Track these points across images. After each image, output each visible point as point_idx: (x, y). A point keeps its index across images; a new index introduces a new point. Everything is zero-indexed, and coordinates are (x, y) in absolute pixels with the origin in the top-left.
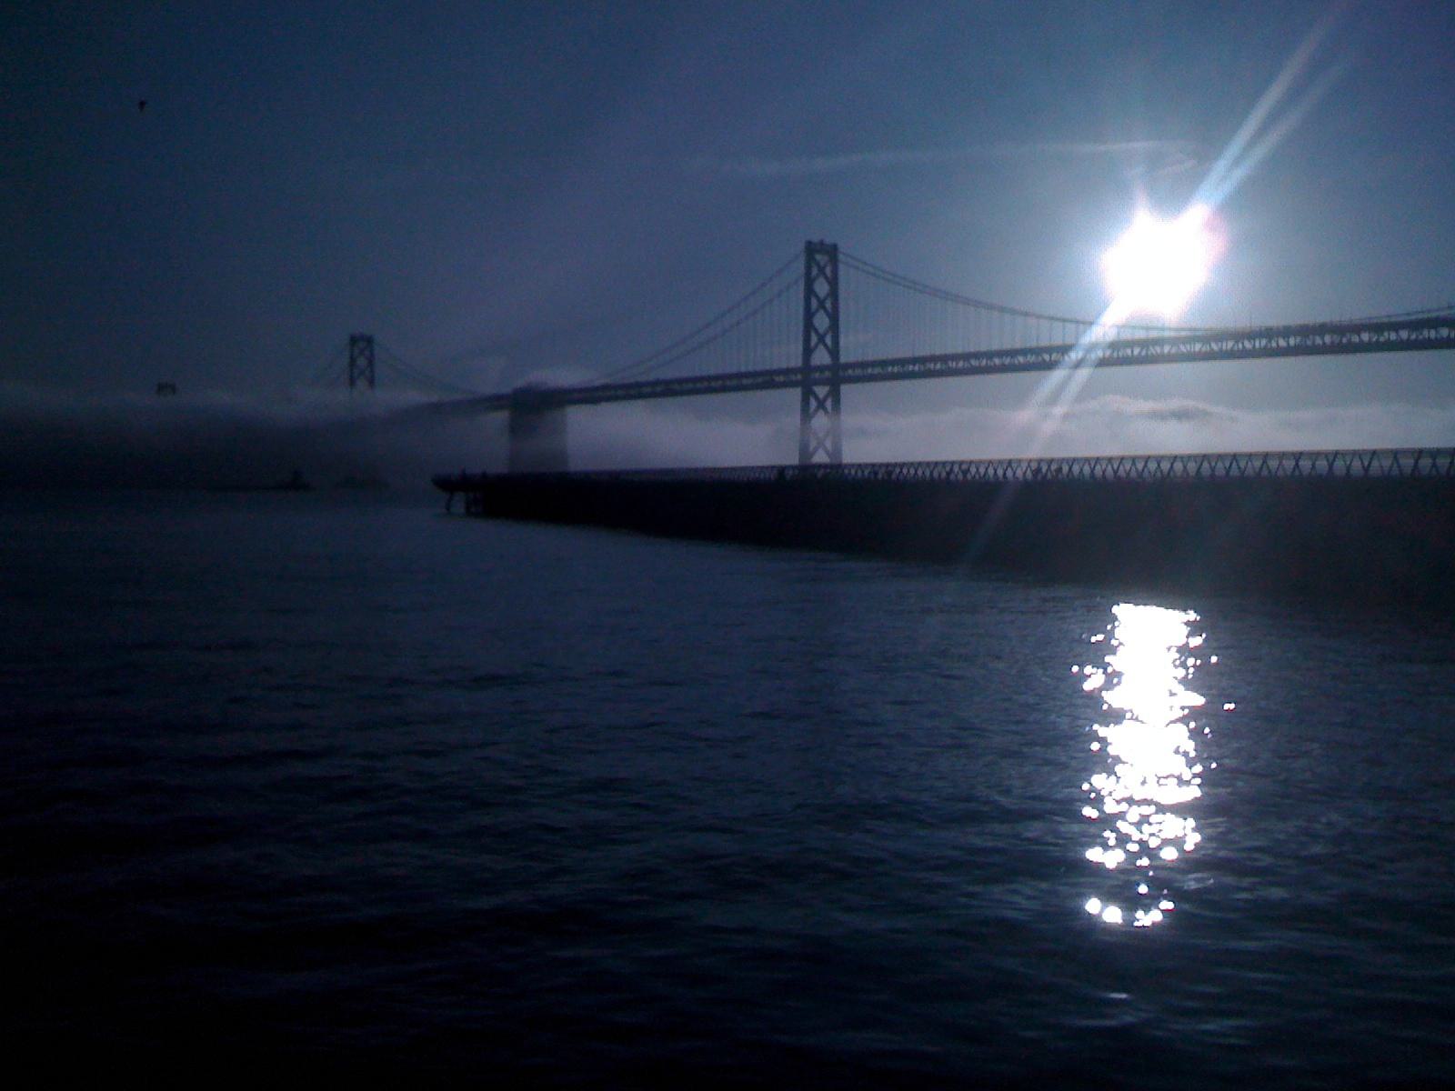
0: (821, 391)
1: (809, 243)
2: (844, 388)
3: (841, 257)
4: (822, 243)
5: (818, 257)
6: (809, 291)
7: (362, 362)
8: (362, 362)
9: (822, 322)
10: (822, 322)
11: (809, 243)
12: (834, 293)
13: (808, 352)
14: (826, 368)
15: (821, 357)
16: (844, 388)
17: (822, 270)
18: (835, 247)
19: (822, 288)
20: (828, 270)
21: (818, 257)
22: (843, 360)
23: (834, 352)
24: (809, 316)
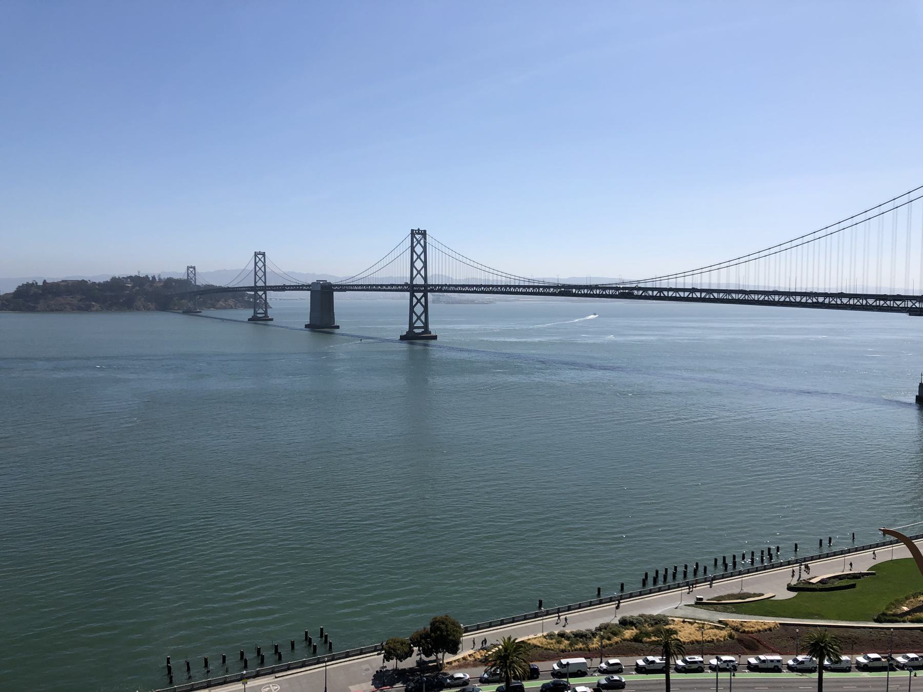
0: (419, 295)
7: (260, 264)
8: (260, 264)
13: (412, 278)
14: (421, 286)
15: (419, 281)
22: (429, 282)
23: (425, 279)
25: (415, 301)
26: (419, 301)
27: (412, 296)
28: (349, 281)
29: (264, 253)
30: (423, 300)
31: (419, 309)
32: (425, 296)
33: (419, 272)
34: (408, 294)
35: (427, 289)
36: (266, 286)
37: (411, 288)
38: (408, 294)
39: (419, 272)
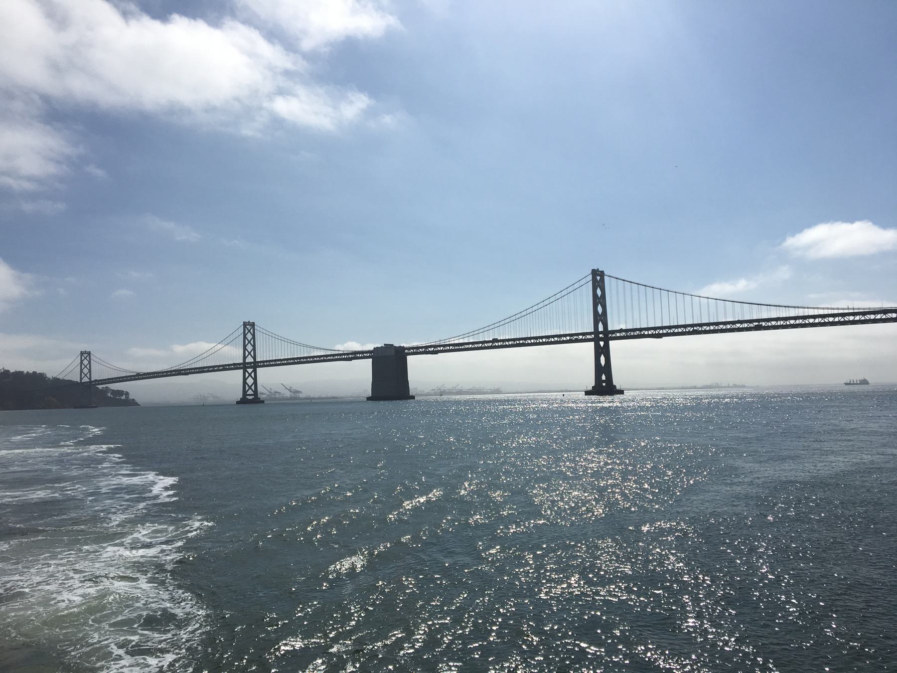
0: (250, 370)
1: (244, 322)
2: (258, 369)
3: (255, 326)
4: (249, 322)
6: (245, 338)
9: (249, 348)
11: (244, 322)
13: (245, 358)
14: (250, 363)
15: (250, 359)
16: (258, 369)
18: (254, 323)
19: (249, 336)
22: (258, 359)
23: (254, 358)
25: (247, 375)
26: (250, 375)
29: (90, 352)
30: (253, 375)
31: (250, 381)
32: (255, 371)
35: (256, 365)
36: (91, 382)
37: (244, 366)
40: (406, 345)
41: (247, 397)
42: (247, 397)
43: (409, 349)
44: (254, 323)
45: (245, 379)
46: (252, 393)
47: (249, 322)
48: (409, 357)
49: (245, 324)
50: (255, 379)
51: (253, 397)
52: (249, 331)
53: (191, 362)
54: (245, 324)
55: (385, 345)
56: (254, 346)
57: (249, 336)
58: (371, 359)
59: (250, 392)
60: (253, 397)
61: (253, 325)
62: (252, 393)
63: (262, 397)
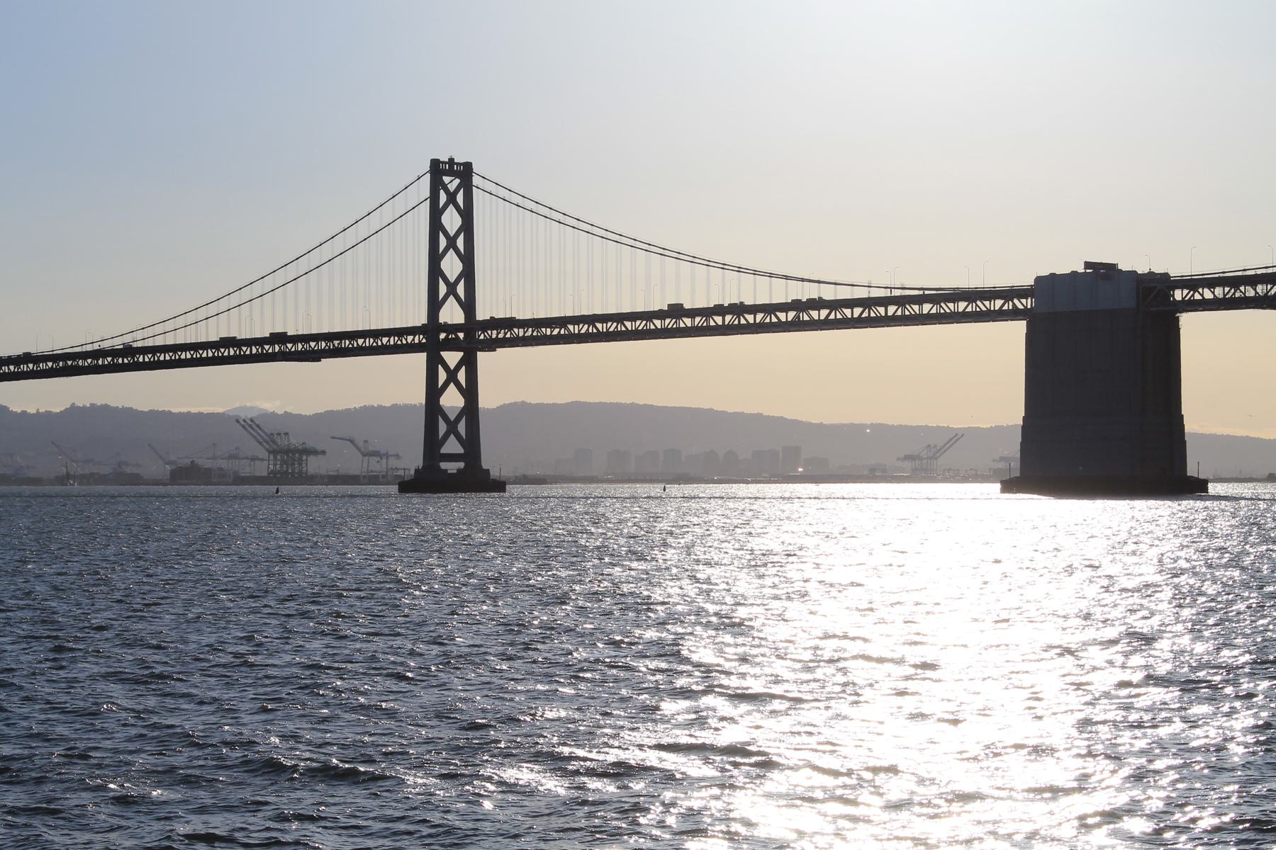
0: (452, 358)
1: (435, 164)
2: (483, 357)
3: (476, 180)
5: (446, 179)
6: (436, 226)
9: (452, 266)
10: (452, 266)
11: (435, 164)
12: (467, 227)
13: (435, 305)
14: (455, 328)
15: (452, 314)
16: (483, 357)
17: (452, 198)
19: (451, 220)
20: (460, 198)
21: (446, 179)
22: (482, 314)
23: (468, 306)
24: (435, 258)
25: (442, 376)
27: (434, 363)
28: (139, 335)
30: (462, 376)
31: (452, 400)
32: (469, 363)
33: (452, 289)
34: (419, 360)
38: (419, 360)
39: (452, 289)
40: (1177, 270)
41: (444, 465)
42: (444, 465)
43: (1192, 283)
44: (468, 166)
45: (434, 392)
46: (459, 450)
47: (451, 161)
48: (1187, 321)
49: (438, 170)
50: (470, 393)
51: (461, 465)
52: (452, 198)
53: (180, 322)
54: (438, 170)
55: (1088, 265)
56: (468, 259)
57: (451, 220)
58: (1020, 327)
59: (452, 446)
60: (461, 465)
61: (465, 172)
62: (459, 450)
63: (492, 460)
